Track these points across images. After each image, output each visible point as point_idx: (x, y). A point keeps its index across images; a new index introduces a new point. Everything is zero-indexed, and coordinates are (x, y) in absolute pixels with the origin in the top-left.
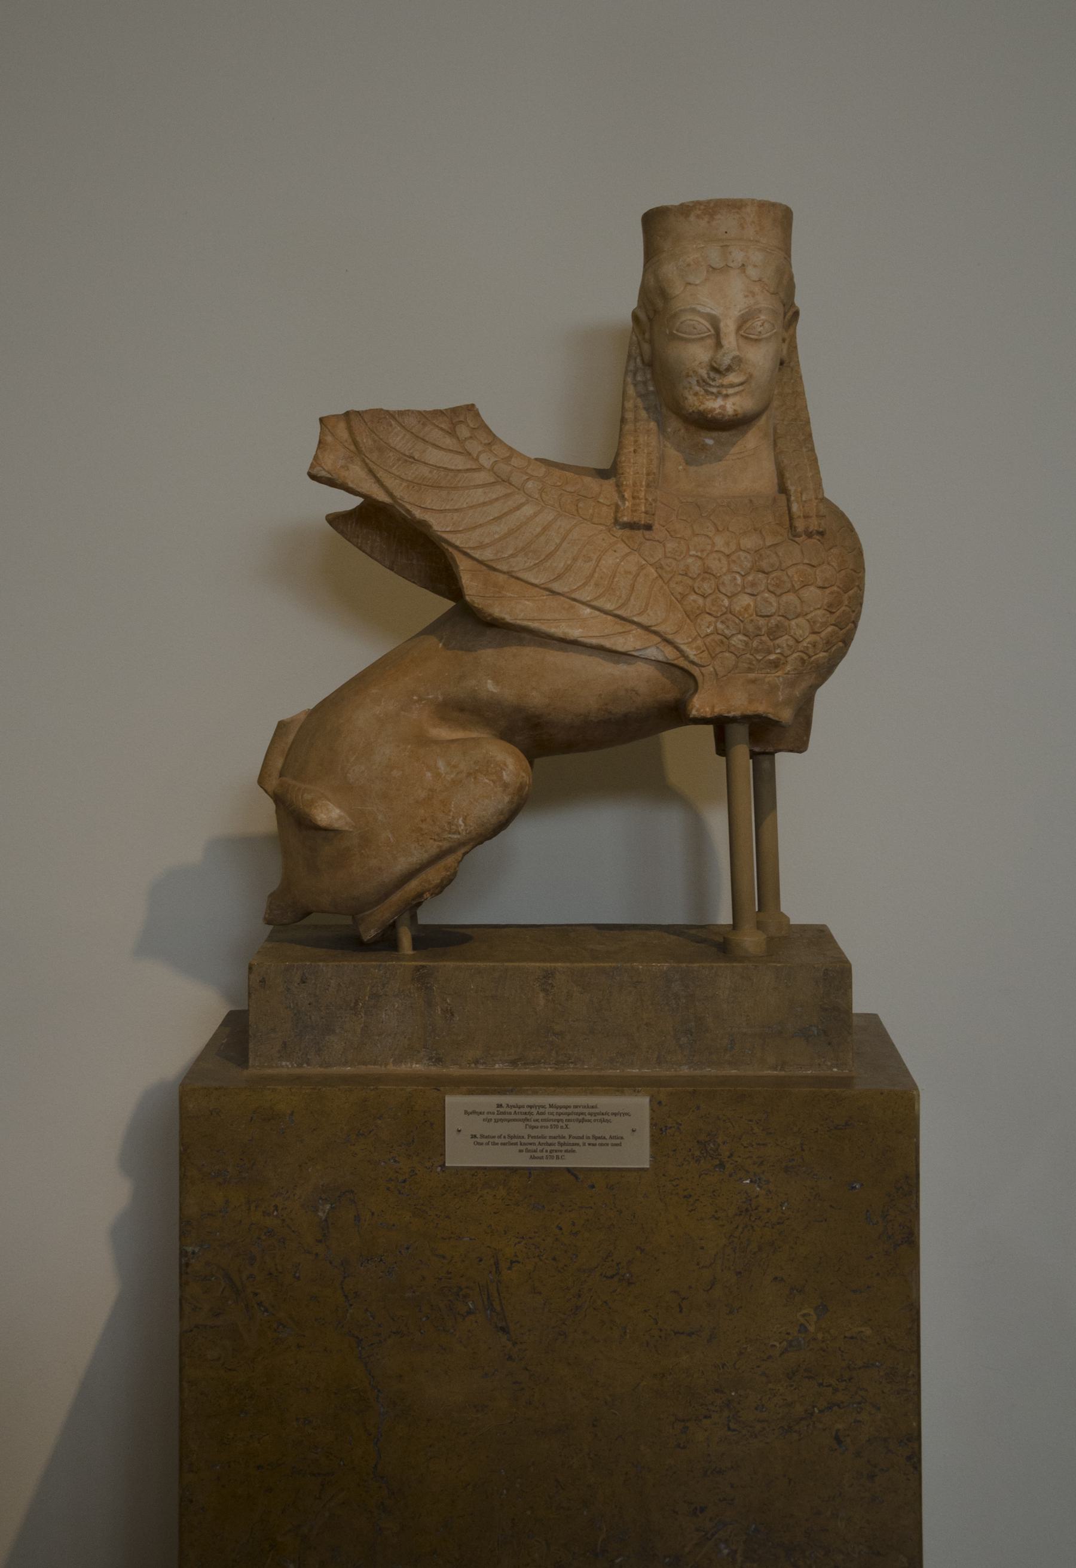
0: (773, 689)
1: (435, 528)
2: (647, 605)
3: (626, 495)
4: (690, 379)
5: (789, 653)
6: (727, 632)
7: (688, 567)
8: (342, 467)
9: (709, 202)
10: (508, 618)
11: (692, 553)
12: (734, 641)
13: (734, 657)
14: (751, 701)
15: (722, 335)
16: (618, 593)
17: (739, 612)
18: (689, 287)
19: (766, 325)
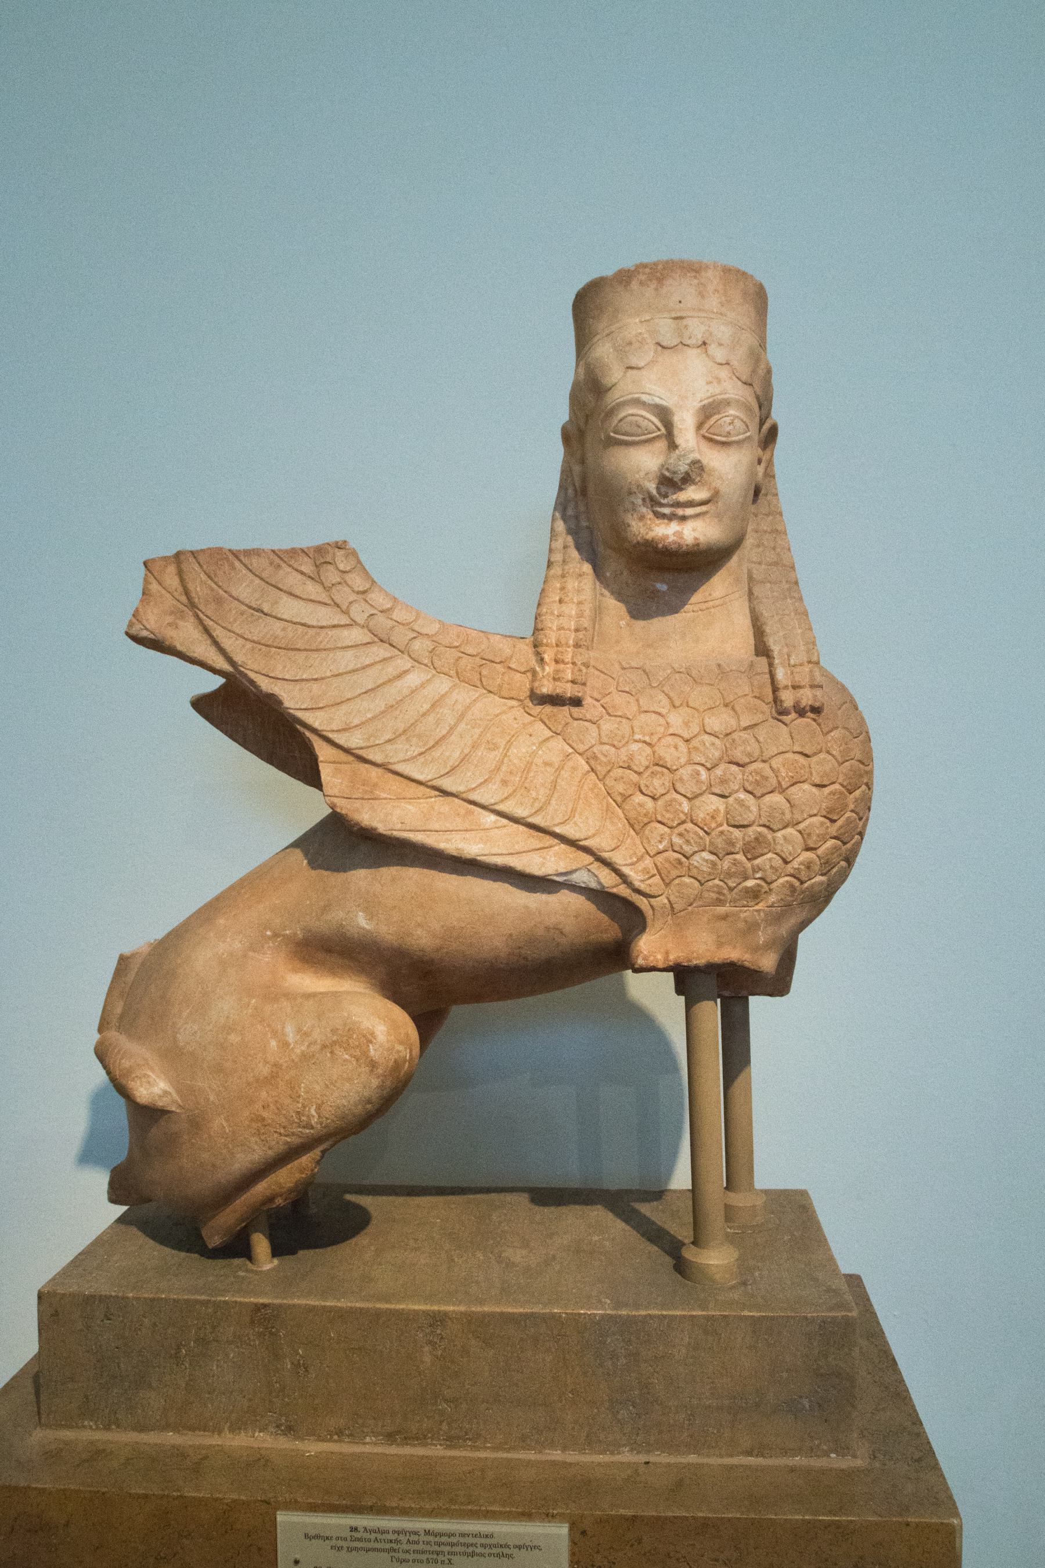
0: (752, 927)
1: (287, 704)
2: (574, 810)
3: (546, 657)
4: (632, 499)
5: (774, 877)
6: (687, 849)
7: (631, 758)
8: (170, 624)
9: (656, 264)
10: (382, 828)
11: (637, 737)
12: (696, 860)
13: (697, 884)
14: (720, 945)
15: (676, 432)
16: (534, 794)
17: (704, 819)
18: (630, 372)
19: (738, 423)
